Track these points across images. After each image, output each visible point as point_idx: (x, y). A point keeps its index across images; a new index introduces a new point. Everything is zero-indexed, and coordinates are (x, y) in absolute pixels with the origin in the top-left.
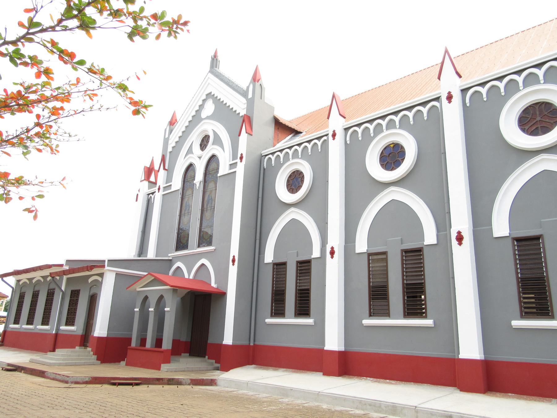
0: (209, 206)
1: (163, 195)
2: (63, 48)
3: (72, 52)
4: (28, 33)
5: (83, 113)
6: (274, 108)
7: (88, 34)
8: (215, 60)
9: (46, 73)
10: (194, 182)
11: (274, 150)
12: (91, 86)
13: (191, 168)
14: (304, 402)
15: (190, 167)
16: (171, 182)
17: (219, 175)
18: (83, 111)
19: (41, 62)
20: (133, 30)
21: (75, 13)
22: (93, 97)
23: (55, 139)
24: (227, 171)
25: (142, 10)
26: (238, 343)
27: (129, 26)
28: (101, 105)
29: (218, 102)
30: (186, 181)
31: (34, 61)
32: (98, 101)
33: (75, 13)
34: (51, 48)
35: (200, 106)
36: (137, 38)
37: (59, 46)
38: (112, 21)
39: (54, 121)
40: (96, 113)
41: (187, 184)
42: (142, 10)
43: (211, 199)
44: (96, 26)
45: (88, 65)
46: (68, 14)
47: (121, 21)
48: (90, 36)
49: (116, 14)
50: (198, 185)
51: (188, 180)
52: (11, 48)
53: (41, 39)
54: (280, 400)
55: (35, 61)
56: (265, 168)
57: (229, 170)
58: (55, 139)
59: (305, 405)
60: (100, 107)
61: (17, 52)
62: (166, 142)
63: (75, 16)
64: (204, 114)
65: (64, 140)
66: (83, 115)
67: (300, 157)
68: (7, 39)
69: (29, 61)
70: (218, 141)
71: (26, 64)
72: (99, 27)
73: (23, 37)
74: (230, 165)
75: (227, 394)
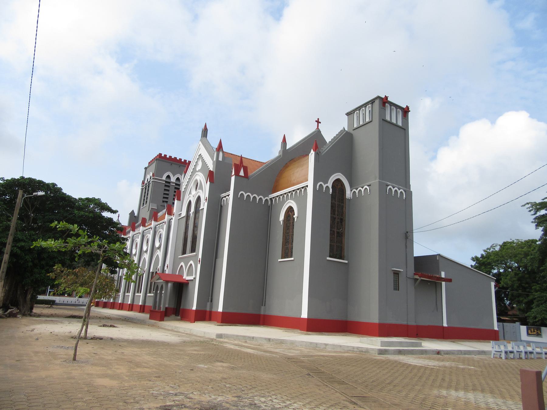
1: (179, 219)
8: (205, 132)
10: (190, 213)
11: (225, 194)
15: (190, 202)
17: (200, 209)
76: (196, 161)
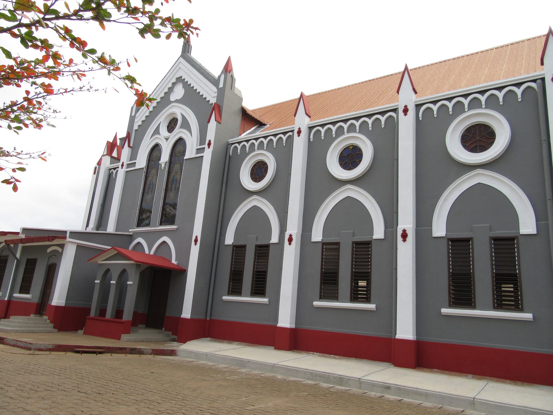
0: (173, 187)
1: (127, 172)
2: (76, 36)
3: (84, 41)
4: (44, 19)
5: (72, 92)
6: (242, 99)
7: (102, 26)
9: (54, 57)
10: (160, 162)
12: (82, 67)
13: (157, 148)
14: (260, 372)
15: (156, 148)
16: (136, 159)
17: (185, 158)
18: (73, 90)
19: (51, 46)
20: (146, 27)
21: (94, 5)
22: (81, 77)
23: (42, 115)
24: (194, 155)
25: (158, 11)
26: (196, 317)
27: (142, 23)
28: (90, 86)
29: (187, 86)
30: (151, 160)
31: (45, 45)
32: (89, 82)
33: (94, 5)
34: (63, 35)
35: (169, 88)
36: (148, 36)
37: (72, 34)
38: (127, 17)
39: (43, 97)
40: (85, 93)
41: (152, 163)
42: (158, 11)
43: (176, 180)
44: (111, 19)
45: (99, 54)
46: (85, 7)
47: (136, 19)
48: (103, 27)
49: (132, 11)
50: (163, 166)
51: (154, 159)
52: (24, 30)
53: (55, 24)
54: (239, 370)
55: (46, 45)
56: (231, 155)
57: (195, 154)
58: (42, 115)
59: (262, 375)
60: (89, 88)
61: (30, 34)
62: (132, 120)
63: (92, 9)
64: (173, 98)
65: (50, 116)
66: (72, 94)
67: (265, 149)
68: (22, 22)
69: (39, 43)
70: (186, 125)
71: (36, 47)
72: (114, 21)
73: (38, 22)
74: (197, 149)
75: (188, 364)
76: (170, 85)
